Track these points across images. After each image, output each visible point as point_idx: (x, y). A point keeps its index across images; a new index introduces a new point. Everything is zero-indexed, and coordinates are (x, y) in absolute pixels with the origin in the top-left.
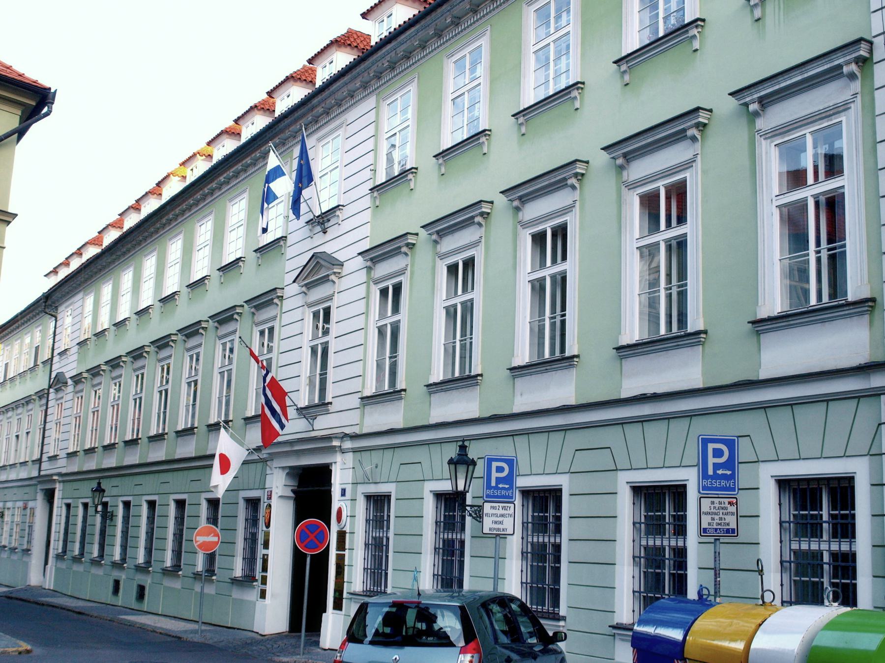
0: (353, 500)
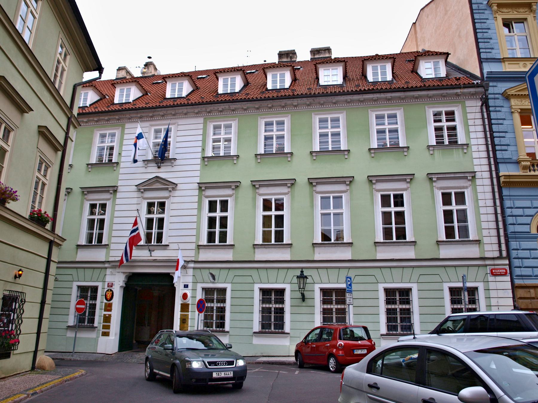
0: (194, 290)
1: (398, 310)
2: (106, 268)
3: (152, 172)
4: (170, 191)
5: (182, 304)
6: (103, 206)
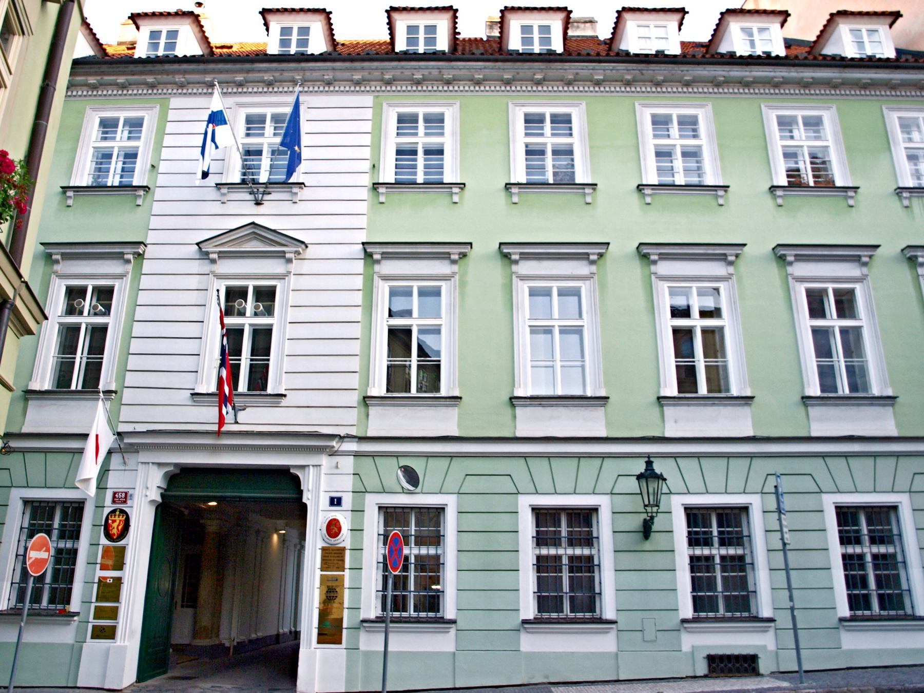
0: (358, 511)
3: (241, 211)
4: (289, 261)
5: (324, 549)
6: (105, 295)
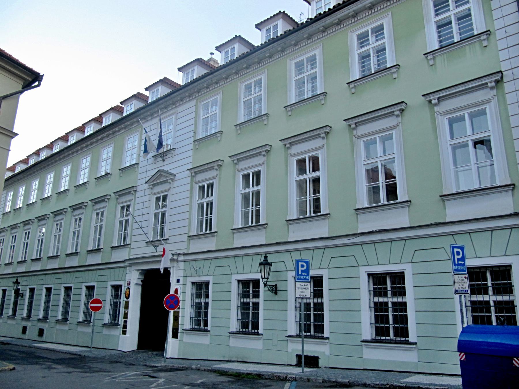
0: (184, 284)
1: (390, 305)
2: (126, 267)
